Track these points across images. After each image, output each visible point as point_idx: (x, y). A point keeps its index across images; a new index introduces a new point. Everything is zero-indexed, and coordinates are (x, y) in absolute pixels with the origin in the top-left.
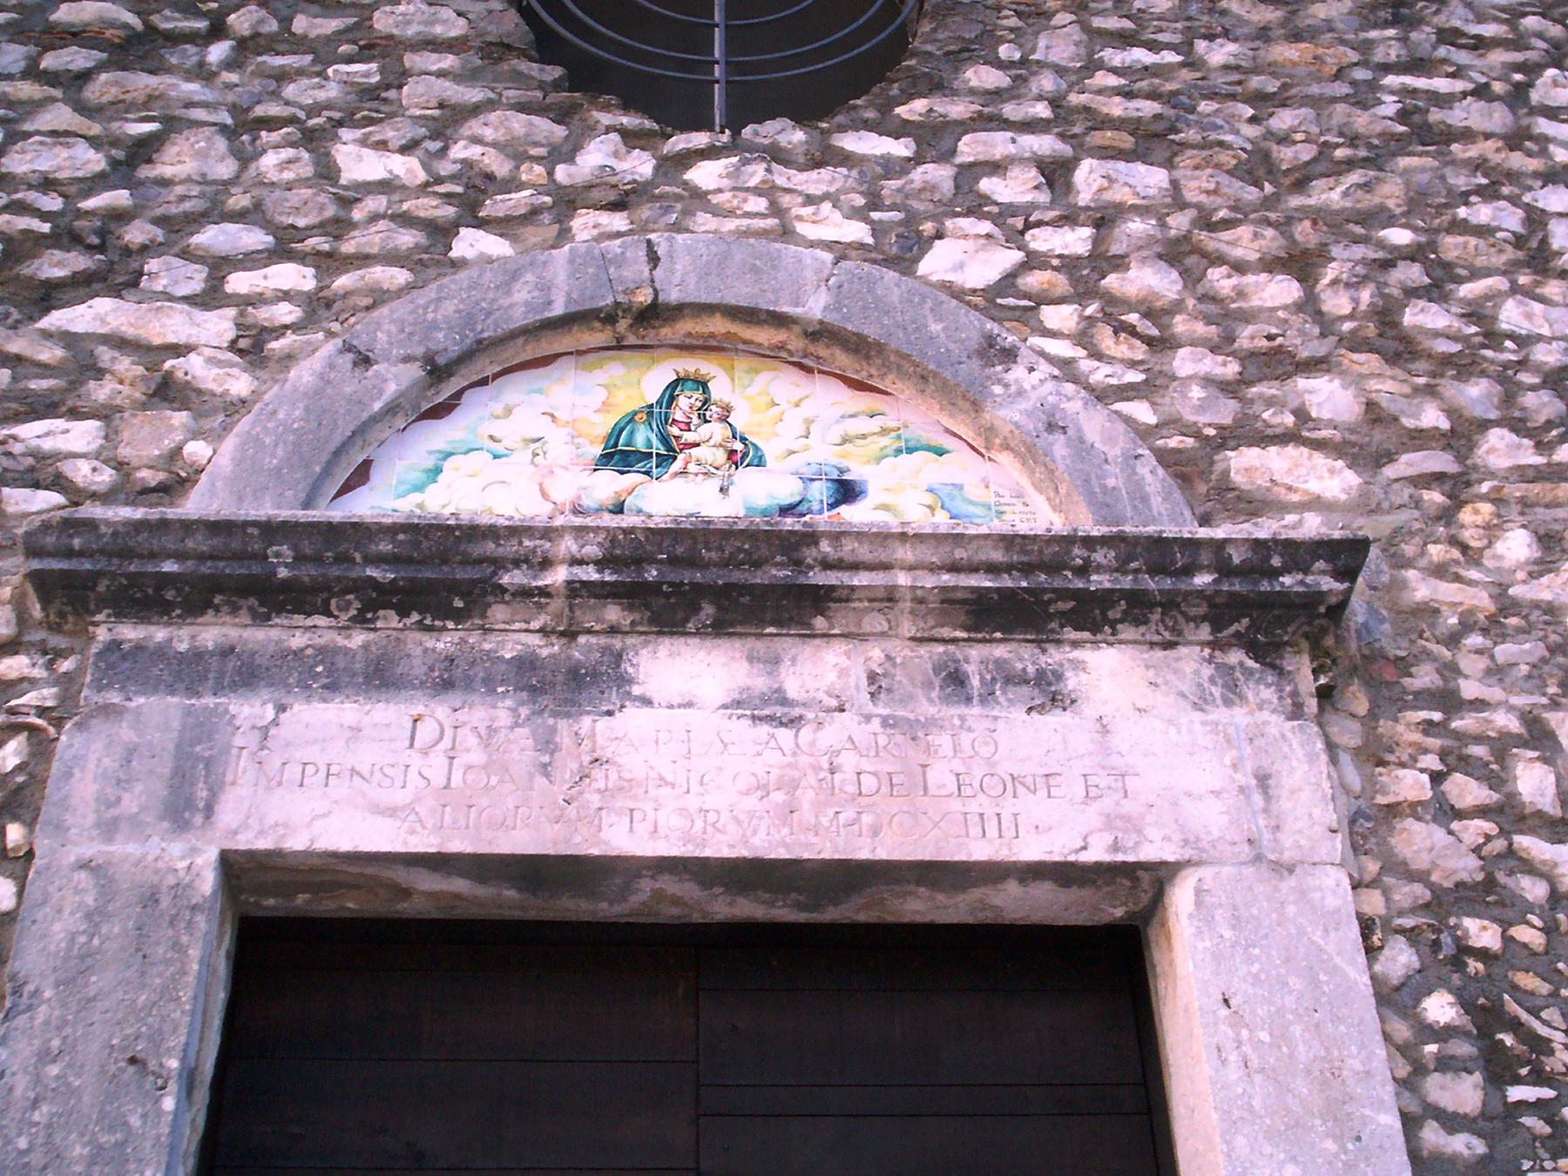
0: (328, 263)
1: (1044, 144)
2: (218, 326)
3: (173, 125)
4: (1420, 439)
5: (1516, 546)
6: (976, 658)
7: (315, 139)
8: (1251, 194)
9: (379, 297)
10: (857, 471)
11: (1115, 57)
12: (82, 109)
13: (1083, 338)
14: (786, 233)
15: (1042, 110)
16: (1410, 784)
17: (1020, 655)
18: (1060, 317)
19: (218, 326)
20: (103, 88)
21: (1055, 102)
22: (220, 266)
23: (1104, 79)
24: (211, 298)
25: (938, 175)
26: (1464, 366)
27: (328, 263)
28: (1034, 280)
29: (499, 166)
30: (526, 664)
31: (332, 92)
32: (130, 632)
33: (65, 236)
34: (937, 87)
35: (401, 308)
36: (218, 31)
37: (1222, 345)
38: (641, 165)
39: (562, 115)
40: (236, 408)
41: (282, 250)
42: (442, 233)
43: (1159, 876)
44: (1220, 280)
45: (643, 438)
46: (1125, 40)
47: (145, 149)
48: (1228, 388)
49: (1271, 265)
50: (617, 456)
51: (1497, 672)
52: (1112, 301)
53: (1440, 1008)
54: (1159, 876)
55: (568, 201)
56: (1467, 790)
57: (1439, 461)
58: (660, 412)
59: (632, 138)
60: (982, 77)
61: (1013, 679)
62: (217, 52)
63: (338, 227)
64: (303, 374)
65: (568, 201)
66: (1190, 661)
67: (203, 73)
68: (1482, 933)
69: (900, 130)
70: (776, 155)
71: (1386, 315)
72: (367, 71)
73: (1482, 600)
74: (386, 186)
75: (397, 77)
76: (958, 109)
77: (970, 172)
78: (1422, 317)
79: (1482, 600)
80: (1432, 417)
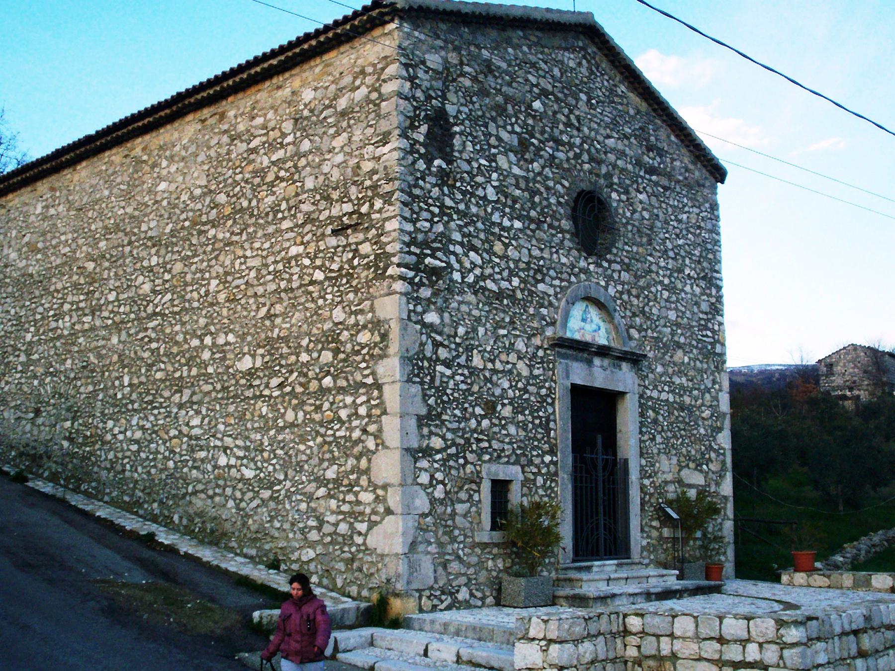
30: (586, 358)
32: (560, 350)
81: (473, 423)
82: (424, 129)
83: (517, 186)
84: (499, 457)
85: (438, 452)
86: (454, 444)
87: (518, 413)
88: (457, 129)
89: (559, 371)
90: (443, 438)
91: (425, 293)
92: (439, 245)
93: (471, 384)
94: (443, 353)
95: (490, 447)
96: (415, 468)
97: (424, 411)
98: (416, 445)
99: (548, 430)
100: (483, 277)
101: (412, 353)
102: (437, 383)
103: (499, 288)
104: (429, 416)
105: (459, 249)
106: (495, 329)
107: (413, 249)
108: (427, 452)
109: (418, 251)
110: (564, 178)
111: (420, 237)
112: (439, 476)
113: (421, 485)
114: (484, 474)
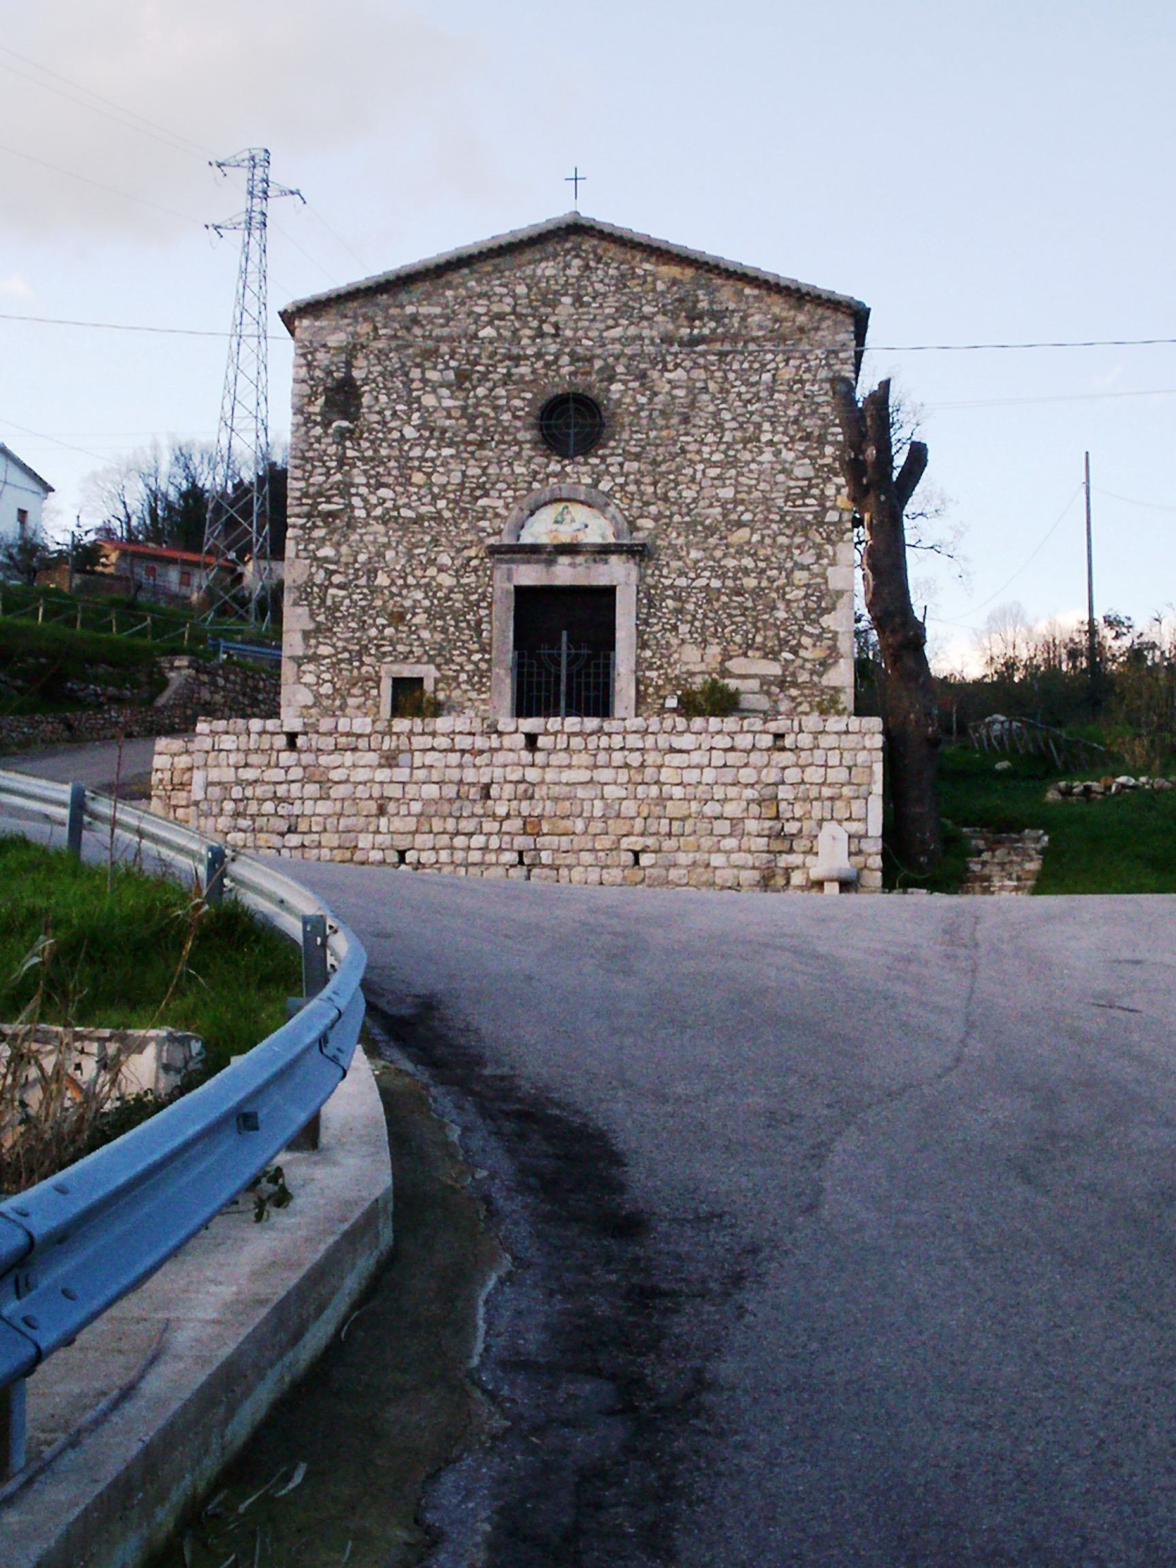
0: (515, 490)
1: (620, 459)
2: (501, 503)
3: (490, 463)
4: (666, 517)
5: (674, 535)
6: (598, 557)
7: (510, 464)
8: (651, 468)
9: (523, 496)
10: (588, 522)
11: (635, 436)
12: (476, 460)
13: (621, 500)
14: (579, 482)
15: (620, 451)
16: (650, 572)
17: (603, 556)
18: (618, 495)
19: (501, 503)
20: (477, 455)
21: (623, 450)
22: (500, 491)
23: (633, 443)
24: (500, 497)
25: (603, 467)
26: (674, 504)
27: (515, 490)
28: (616, 488)
29: (537, 469)
31: (512, 454)
33: (478, 487)
34: (605, 446)
35: (526, 500)
36: (493, 439)
37: (640, 500)
38: (558, 468)
39: (547, 457)
40: (506, 518)
41: (508, 488)
42: (530, 483)
43: (615, 587)
44: (642, 487)
45: (559, 519)
46: (637, 432)
47: (486, 467)
48: (641, 508)
49: (651, 484)
50: (556, 522)
51: (666, 554)
52: (626, 492)
53: (645, 601)
54: (615, 587)
55: (548, 476)
56: (657, 572)
57: (666, 521)
58: (562, 514)
59: (558, 462)
60: (612, 444)
61: (601, 560)
62: (493, 444)
63: (516, 483)
64: (514, 513)
65: (548, 476)
66: (624, 557)
67: (492, 450)
68: (653, 591)
69: (597, 456)
70: (579, 463)
71: (666, 494)
72: (516, 448)
73: (666, 544)
74: (522, 474)
75: (521, 449)
76: (607, 452)
77: (608, 466)
78: (672, 494)
79: (666, 544)
80: (668, 513)
81: (373, 632)
82: (321, 401)
83: (449, 417)
84: (406, 658)
85: (325, 657)
86: (345, 649)
87: (436, 618)
88: (366, 388)
89: (497, 575)
90: (333, 646)
91: (319, 533)
92: (335, 492)
93: (372, 600)
94: (337, 579)
95: (395, 650)
96: (299, 670)
97: (312, 626)
98: (301, 654)
99: (479, 633)
100: (396, 508)
101: (300, 582)
102: (329, 602)
103: (418, 513)
104: (318, 629)
105: (363, 490)
106: (410, 550)
107: (304, 501)
108: (315, 658)
109: (310, 501)
110: (523, 391)
111: (312, 490)
112: (327, 676)
113: (305, 684)
114: (383, 674)
